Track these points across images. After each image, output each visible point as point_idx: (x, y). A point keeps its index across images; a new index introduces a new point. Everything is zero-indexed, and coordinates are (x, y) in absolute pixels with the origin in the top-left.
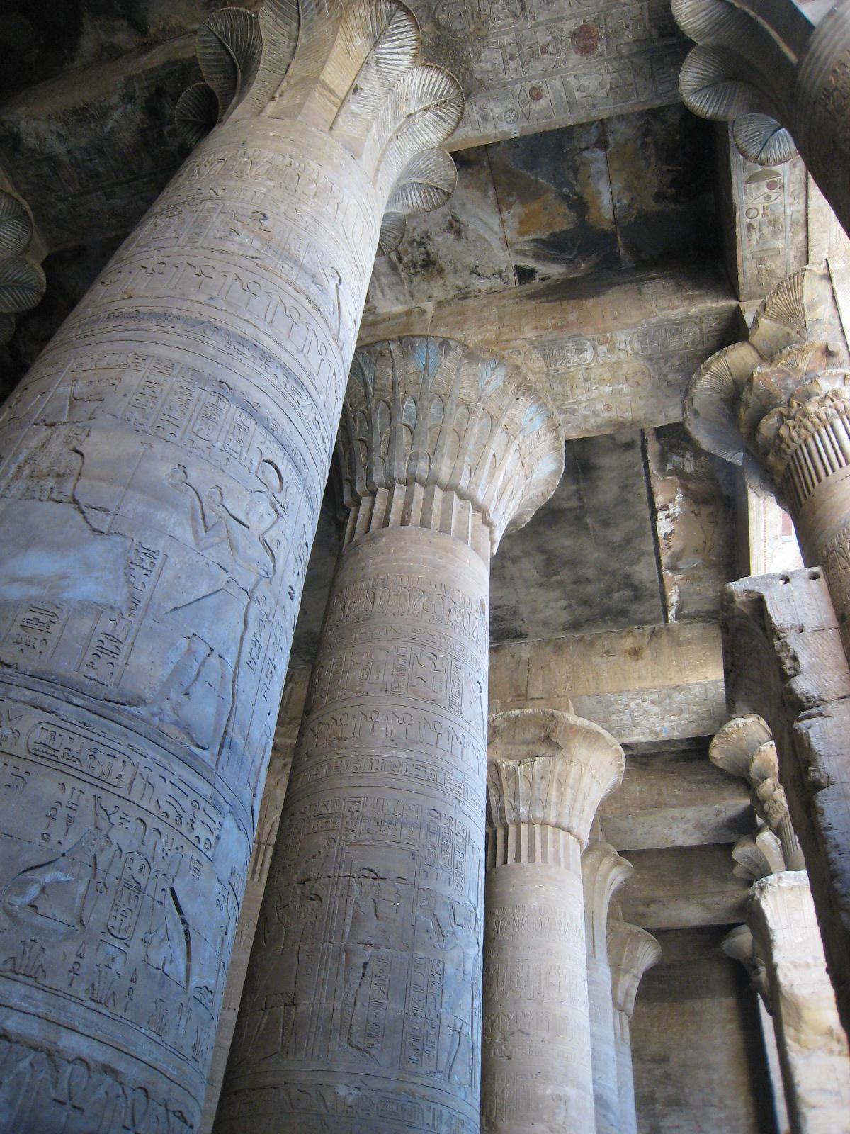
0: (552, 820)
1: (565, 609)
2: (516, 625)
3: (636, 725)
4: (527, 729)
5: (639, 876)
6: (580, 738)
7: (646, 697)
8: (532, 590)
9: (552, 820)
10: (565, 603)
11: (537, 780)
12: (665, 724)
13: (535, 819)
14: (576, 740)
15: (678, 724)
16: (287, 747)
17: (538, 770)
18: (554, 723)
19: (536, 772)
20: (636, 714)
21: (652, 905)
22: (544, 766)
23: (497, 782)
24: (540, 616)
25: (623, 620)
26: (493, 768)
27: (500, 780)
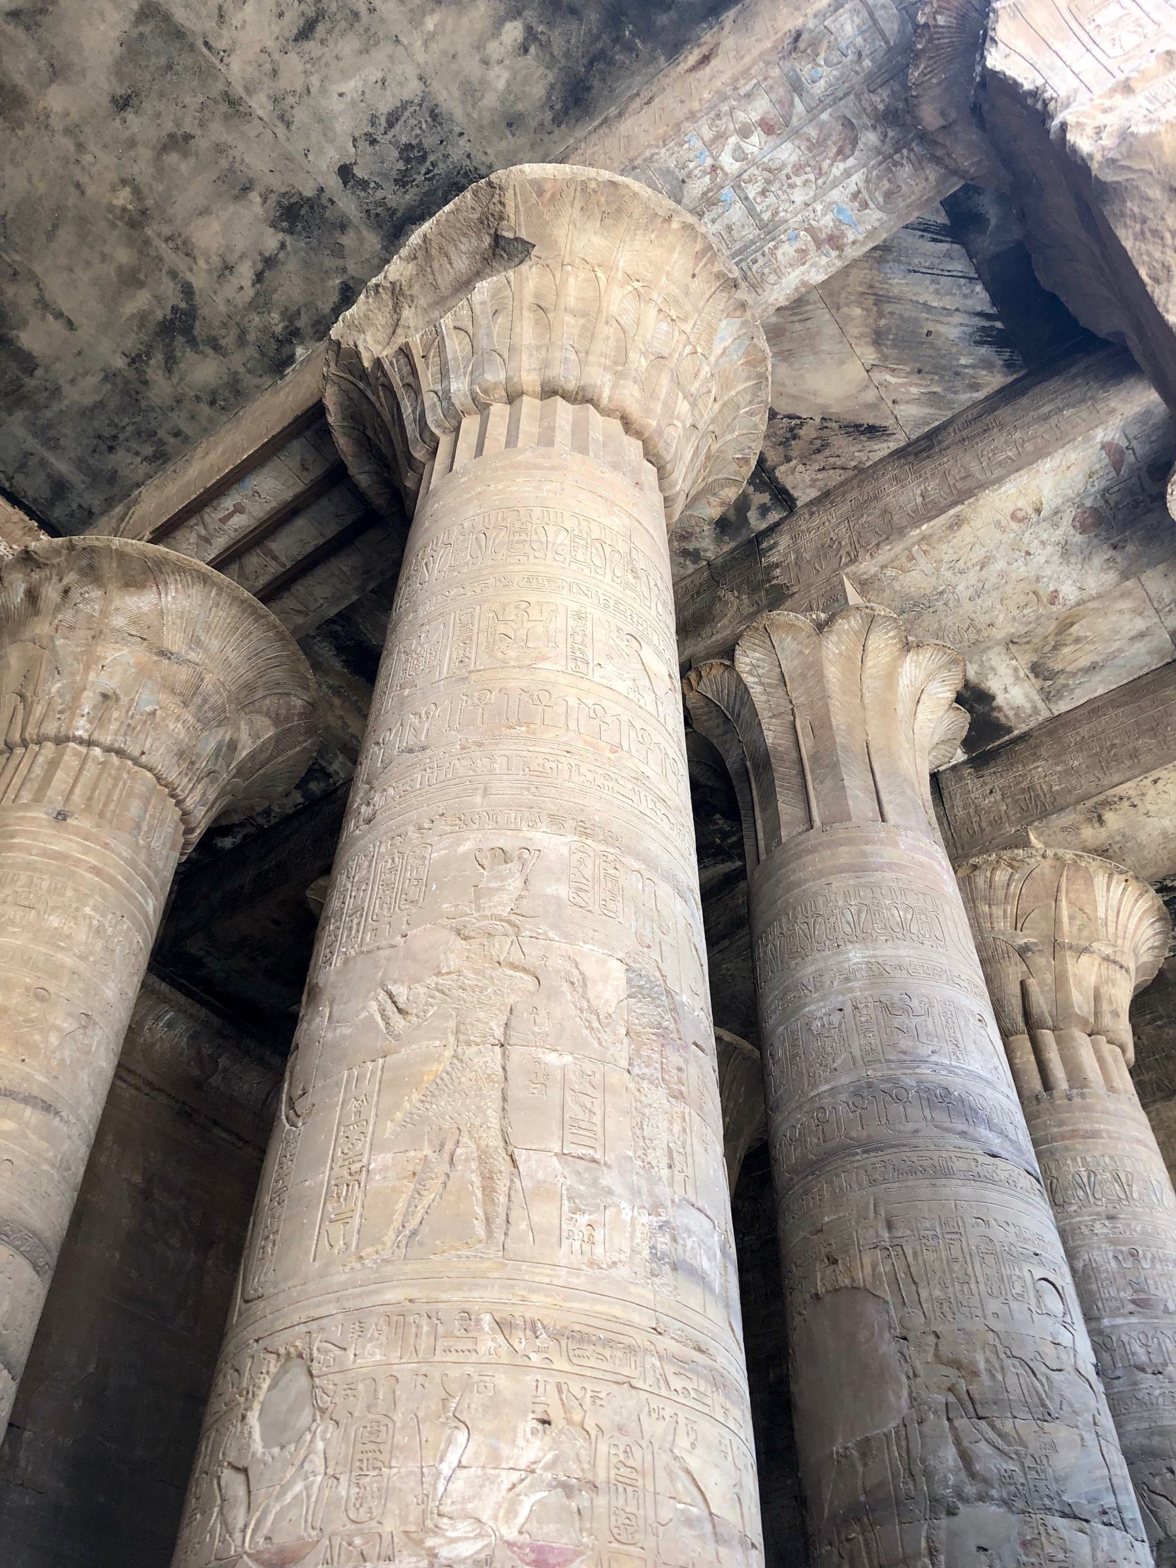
0: (530, 379)
1: (526, 51)
2: (457, 152)
3: (770, 229)
4: (451, 249)
5: (1058, 768)
6: (571, 212)
7: (741, 116)
8: (430, 23)
9: (530, 379)
10: (513, 31)
11: (483, 322)
12: (835, 194)
13: (485, 392)
14: (565, 220)
15: (867, 181)
16: (57, 552)
17: (483, 303)
18: (496, 199)
19: (478, 309)
20: (752, 191)
21: (1108, 816)
22: (496, 293)
23: (410, 380)
24: (490, 100)
25: (663, 19)
26: (403, 360)
27: (414, 372)
